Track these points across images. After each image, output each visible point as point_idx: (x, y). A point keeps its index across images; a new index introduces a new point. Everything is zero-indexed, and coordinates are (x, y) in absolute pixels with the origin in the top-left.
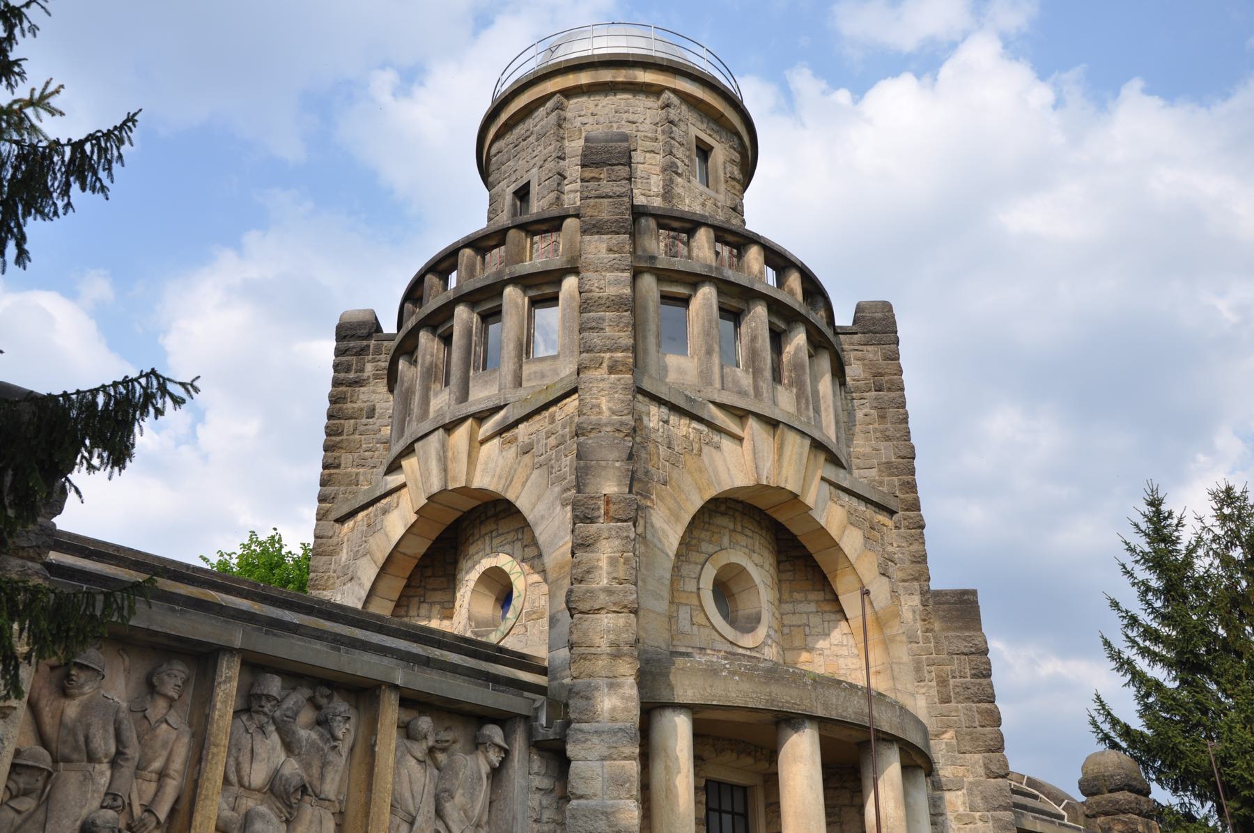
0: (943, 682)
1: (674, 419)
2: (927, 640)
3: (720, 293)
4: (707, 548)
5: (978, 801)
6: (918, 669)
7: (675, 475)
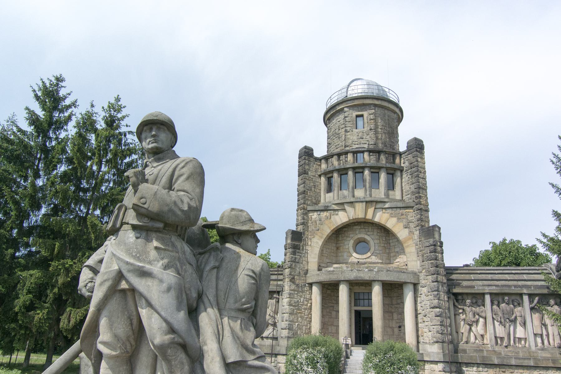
0: (423, 256)
1: (322, 213)
3: (339, 172)
4: (351, 236)
5: (430, 290)
6: (418, 253)
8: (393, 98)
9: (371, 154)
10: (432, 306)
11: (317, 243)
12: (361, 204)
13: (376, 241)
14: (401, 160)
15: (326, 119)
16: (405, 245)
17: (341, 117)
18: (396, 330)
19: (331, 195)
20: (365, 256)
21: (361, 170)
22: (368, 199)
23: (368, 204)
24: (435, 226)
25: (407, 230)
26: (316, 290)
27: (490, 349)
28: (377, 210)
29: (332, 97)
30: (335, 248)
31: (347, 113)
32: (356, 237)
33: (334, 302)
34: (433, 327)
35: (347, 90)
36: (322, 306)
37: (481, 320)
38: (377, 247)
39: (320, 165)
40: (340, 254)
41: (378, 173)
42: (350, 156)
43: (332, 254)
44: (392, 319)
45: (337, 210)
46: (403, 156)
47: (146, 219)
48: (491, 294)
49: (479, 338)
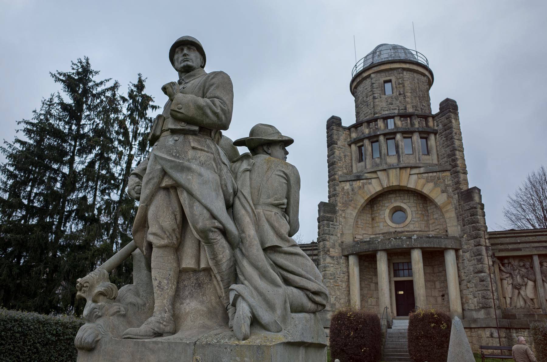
0: (463, 220)
1: (354, 183)
2: (459, 208)
3: (369, 140)
4: (386, 205)
5: (473, 255)
6: (458, 218)
7: (355, 197)
8: (421, 60)
9: (402, 119)
10: (476, 270)
11: (351, 214)
12: (394, 170)
13: (413, 209)
14: (434, 123)
15: (353, 88)
16: (444, 210)
17: (368, 82)
18: (440, 299)
19: (362, 164)
20: (402, 225)
21: (392, 136)
22: (401, 166)
23: (402, 170)
24: (475, 188)
25: (445, 195)
26: (352, 260)
27: (542, 313)
28: (411, 176)
29: (357, 65)
30: (370, 219)
31: (374, 79)
32: (392, 206)
33: (372, 273)
34: (479, 292)
35: (373, 55)
36: (360, 278)
37: (530, 283)
38: (414, 215)
39: (350, 135)
40: (376, 225)
41: (411, 137)
42: (380, 123)
43: (368, 225)
44: (435, 288)
45: (370, 179)
46: (436, 118)
47: (183, 123)
48: (540, 256)
49: (529, 303)
